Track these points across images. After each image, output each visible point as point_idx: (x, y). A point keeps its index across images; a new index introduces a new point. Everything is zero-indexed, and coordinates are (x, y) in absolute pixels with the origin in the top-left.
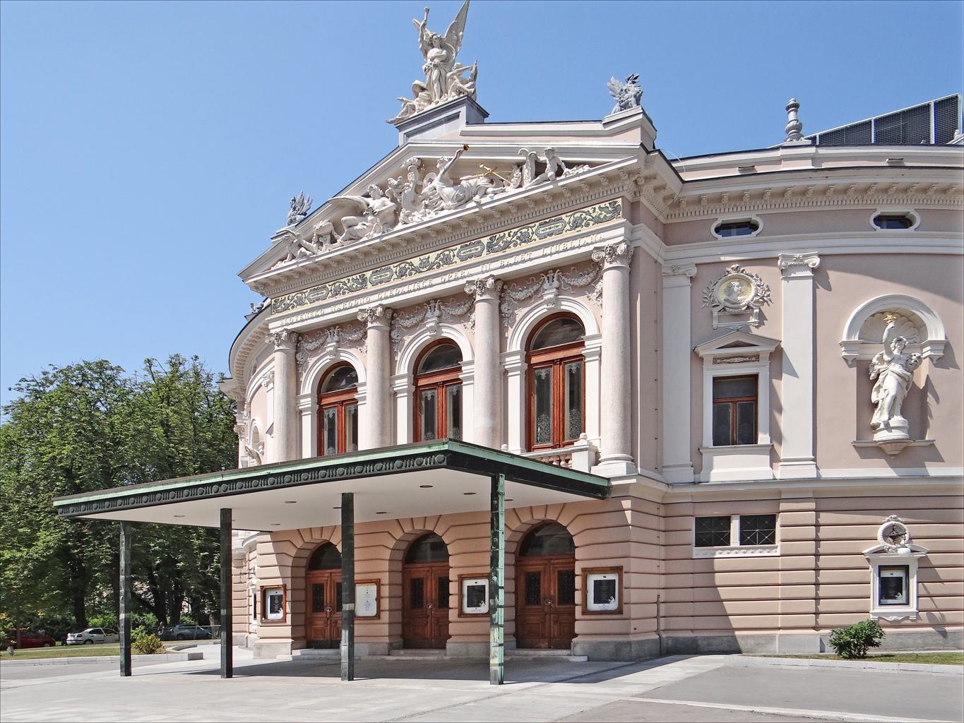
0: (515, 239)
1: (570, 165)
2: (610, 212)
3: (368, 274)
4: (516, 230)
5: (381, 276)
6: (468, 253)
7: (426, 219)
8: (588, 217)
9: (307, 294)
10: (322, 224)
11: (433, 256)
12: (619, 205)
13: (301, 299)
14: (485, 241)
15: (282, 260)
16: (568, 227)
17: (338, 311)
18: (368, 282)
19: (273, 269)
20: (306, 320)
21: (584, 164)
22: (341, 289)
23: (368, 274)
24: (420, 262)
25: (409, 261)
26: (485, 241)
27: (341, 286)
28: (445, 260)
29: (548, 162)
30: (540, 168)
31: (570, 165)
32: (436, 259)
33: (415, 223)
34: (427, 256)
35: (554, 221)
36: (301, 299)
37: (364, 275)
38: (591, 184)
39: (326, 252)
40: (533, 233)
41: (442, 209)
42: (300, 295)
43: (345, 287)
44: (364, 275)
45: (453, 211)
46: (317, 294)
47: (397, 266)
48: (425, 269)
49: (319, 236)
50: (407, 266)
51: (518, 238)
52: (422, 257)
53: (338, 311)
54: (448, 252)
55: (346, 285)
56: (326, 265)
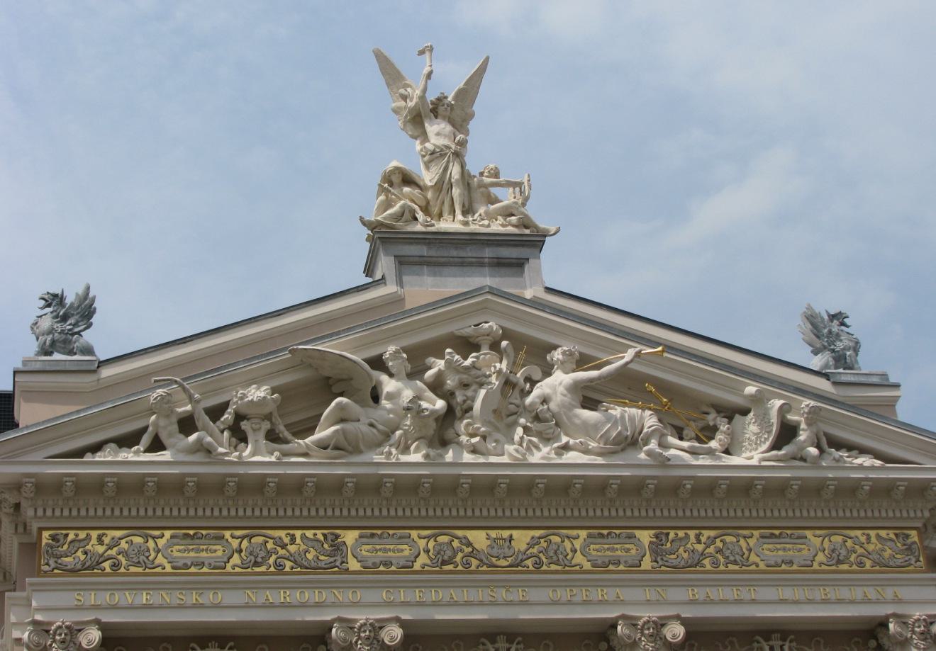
0: (711, 550)
1: (837, 444)
2: (901, 552)
3: (350, 537)
4: (712, 533)
5: (385, 551)
6: (608, 553)
7: (536, 457)
8: (860, 551)
9: (161, 542)
10: (257, 393)
11: (522, 538)
12: (914, 543)
13: (142, 551)
14: (645, 537)
15: (127, 441)
16: (821, 557)
17: (263, 606)
18: (350, 555)
19: (88, 457)
20: (160, 607)
21: (863, 451)
22: (270, 553)
23: (350, 537)
24: (489, 542)
25: (460, 533)
26: (645, 537)
27: (270, 545)
28: (551, 554)
29: (803, 426)
30: (787, 433)
31: (837, 444)
32: (531, 546)
33: (505, 459)
34: (506, 534)
35: (791, 536)
36: (142, 551)
37: (337, 537)
38: (884, 490)
39: (257, 457)
40: (750, 550)
41: (566, 448)
42: (138, 540)
43: (282, 552)
44: (337, 537)
45: (600, 460)
46: (198, 551)
47: (429, 537)
48: (503, 563)
49: (239, 417)
50: (456, 544)
51: (719, 551)
52: (493, 534)
53: (263, 606)
54: (556, 539)
55: (284, 546)
56: (254, 487)
